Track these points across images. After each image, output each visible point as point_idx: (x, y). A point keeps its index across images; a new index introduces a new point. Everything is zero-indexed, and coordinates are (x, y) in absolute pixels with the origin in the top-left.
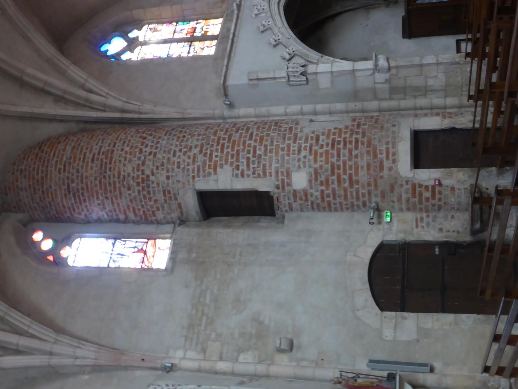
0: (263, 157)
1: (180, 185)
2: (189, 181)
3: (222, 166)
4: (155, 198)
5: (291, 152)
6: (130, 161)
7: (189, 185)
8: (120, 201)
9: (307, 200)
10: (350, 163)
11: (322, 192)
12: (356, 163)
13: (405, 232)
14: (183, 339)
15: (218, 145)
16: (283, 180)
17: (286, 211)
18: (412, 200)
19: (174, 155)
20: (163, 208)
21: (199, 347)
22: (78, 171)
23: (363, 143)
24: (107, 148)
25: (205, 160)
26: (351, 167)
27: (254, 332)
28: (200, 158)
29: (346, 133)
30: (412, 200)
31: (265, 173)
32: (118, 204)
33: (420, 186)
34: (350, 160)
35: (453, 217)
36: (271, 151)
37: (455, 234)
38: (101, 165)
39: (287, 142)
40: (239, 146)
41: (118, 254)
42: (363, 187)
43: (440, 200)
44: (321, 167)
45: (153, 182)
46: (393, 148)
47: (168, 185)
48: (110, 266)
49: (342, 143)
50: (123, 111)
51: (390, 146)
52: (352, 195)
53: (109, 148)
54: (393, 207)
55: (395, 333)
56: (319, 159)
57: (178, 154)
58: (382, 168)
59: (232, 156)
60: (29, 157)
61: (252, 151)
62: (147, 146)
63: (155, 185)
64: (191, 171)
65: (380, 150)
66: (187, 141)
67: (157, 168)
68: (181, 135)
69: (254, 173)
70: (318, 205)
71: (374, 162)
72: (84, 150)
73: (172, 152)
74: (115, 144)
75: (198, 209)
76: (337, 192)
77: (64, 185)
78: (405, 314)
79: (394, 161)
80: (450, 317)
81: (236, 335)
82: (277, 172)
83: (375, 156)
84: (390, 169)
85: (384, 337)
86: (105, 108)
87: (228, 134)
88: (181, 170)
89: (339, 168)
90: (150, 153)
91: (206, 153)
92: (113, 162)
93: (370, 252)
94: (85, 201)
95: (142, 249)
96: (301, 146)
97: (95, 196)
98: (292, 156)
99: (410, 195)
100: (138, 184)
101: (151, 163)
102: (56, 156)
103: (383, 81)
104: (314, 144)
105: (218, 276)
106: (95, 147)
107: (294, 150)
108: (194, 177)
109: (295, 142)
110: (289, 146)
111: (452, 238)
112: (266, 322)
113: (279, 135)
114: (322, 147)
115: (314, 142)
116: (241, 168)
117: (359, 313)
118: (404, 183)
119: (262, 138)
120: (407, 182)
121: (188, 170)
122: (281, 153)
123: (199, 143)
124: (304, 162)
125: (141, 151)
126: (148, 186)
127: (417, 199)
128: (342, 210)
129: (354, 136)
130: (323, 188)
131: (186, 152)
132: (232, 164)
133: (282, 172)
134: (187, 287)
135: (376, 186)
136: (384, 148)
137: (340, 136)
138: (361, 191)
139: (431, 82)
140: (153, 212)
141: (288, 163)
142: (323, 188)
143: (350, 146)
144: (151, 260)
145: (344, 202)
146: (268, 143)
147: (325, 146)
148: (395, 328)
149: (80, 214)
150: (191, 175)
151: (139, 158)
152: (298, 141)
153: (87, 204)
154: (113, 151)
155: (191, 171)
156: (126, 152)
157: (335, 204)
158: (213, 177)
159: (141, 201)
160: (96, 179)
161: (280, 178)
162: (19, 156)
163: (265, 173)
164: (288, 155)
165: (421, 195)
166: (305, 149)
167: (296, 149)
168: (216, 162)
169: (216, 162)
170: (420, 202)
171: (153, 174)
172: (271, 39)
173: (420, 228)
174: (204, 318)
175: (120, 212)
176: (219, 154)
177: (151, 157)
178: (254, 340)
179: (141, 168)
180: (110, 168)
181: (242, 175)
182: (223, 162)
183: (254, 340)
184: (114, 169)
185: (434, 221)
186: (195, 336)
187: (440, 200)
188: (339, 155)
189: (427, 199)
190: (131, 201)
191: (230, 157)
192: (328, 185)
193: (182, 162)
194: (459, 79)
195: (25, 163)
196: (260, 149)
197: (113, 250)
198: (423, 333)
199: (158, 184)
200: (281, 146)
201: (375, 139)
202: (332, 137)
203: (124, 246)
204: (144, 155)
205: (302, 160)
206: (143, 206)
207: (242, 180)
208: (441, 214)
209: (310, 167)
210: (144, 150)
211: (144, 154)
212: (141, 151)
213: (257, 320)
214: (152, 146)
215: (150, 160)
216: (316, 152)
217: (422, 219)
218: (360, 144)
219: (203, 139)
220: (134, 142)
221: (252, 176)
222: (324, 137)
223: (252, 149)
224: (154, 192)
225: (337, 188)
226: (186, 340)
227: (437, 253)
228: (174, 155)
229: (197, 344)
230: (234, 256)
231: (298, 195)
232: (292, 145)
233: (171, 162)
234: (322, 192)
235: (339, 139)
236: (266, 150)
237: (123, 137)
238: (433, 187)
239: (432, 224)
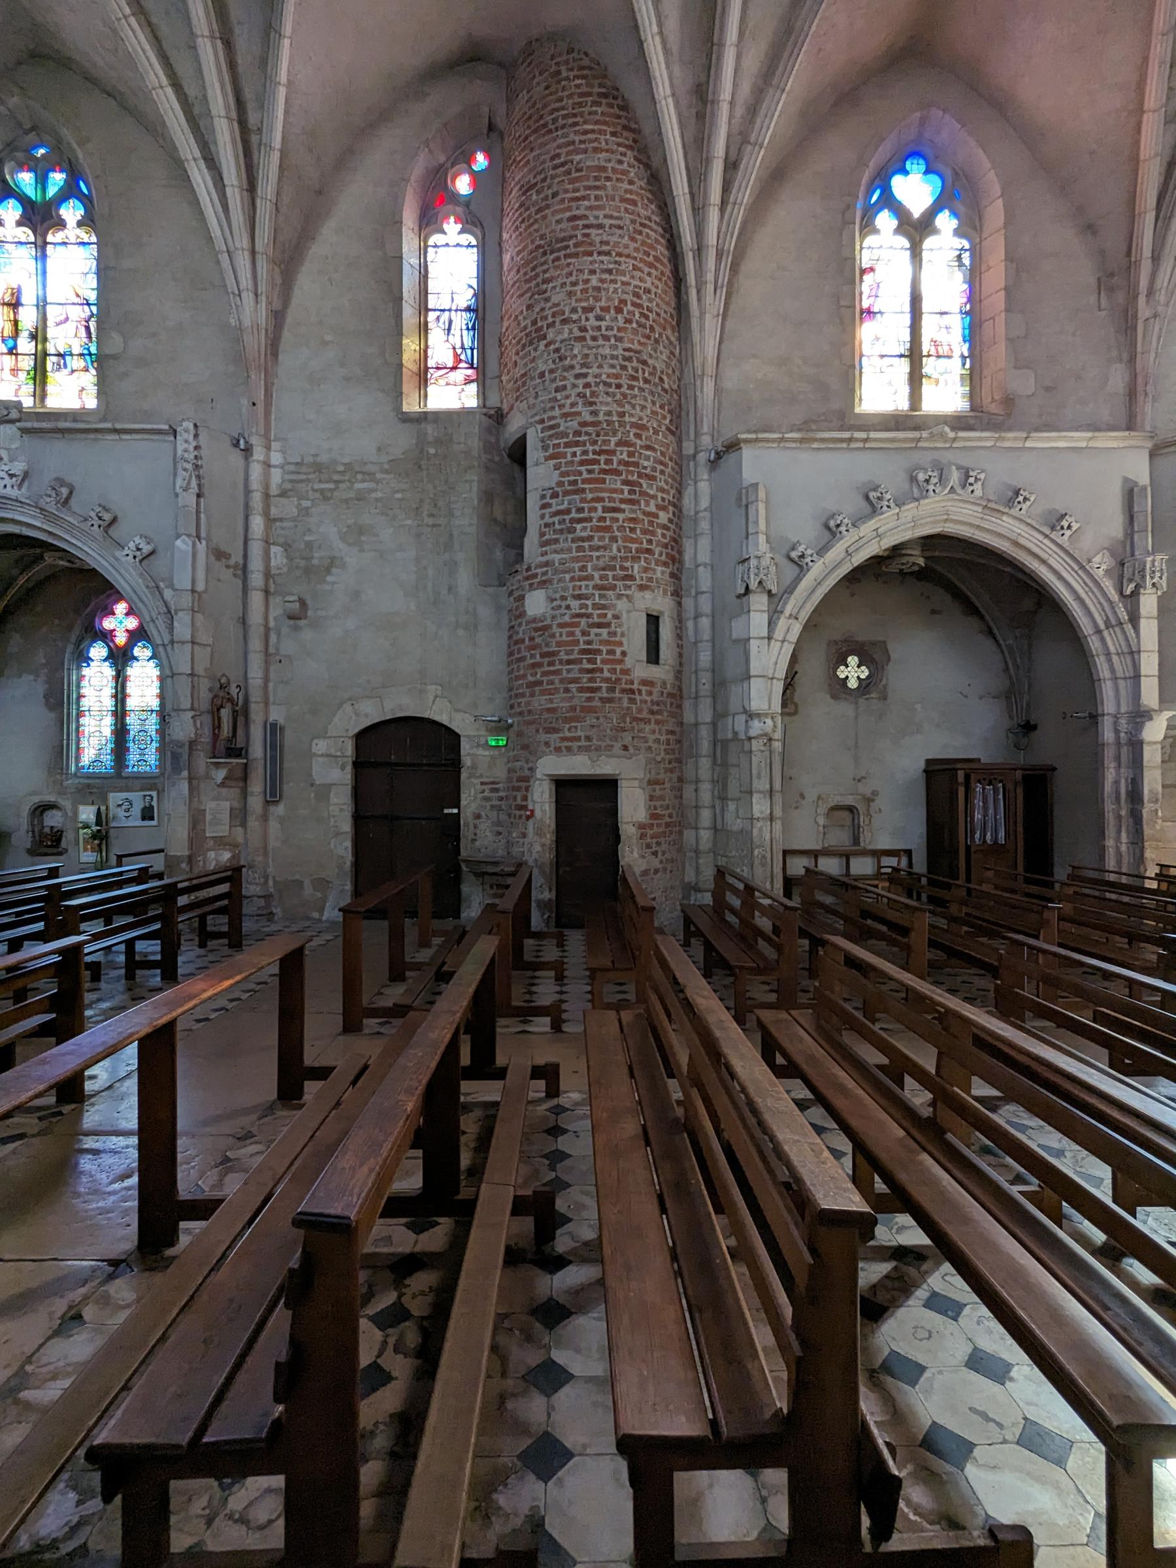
0: (570, 536)
1: (532, 401)
3: (557, 467)
5: (578, 583)
6: (570, 294)
10: (557, 681)
11: (523, 641)
12: (557, 690)
13: (474, 767)
14: (299, 460)
15: (595, 452)
19: (577, 376)
21: (288, 486)
22: (554, 195)
23: (589, 699)
24: (598, 239)
25: (567, 435)
26: (551, 682)
27: (315, 562)
29: (613, 671)
33: (527, 789)
34: (561, 681)
35: (500, 834)
36: (579, 549)
37: (471, 836)
38: (563, 239)
39: (596, 575)
40: (591, 490)
41: (450, 322)
42: (528, 703)
45: (535, 350)
46: (579, 747)
47: (532, 379)
48: (430, 313)
49: (590, 666)
50: (700, 250)
51: (583, 743)
53: (598, 245)
55: (322, 755)
56: (564, 631)
57: (581, 382)
58: (548, 731)
59: (575, 482)
60: (583, 77)
61: (582, 515)
62: (599, 318)
64: (550, 414)
65: (576, 727)
66: (607, 393)
68: (624, 381)
69: (546, 525)
71: (557, 719)
72: (593, 193)
73: (584, 371)
74: (608, 253)
76: (522, 664)
78: (349, 768)
79: (558, 750)
80: (347, 826)
81: (307, 538)
82: (547, 564)
83: (567, 720)
84: (547, 744)
85: (315, 741)
86: (698, 210)
87: (621, 468)
88: (554, 394)
90: (583, 329)
91: (580, 435)
92: (569, 260)
93: (443, 719)
95: (461, 361)
96: (587, 599)
98: (571, 585)
101: (566, 336)
102: (583, 138)
104: (590, 620)
105: (399, 496)
106: (601, 214)
107: (580, 588)
108: (542, 421)
109: (596, 587)
110: (589, 578)
111: (466, 833)
112: (329, 579)
113: (614, 558)
114: (584, 633)
115: (596, 620)
116: (554, 501)
117: (347, 707)
119: (608, 529)
120: (531, 769)
122: (577, 565)
123: (601, 417)
124: (560, 606)
125: (587, 310)
129: (604, 685)
131: (585, 396)
132: (561, 484)
134: (379, 449)
136: (579, 733)
137: (604, 662)
139: (732, 806)
141: (560, 580)
143: (585, 680)
144: (442, 382)
146: (596, 542)
147: (586, 638)
148: (328, 756)
150: (545, 416)
151: (574, 310)
152: (597, 593)
154: (590, 254)
155: (550, 414)
156: (587, 281)
158: (542, 455)
160: (542, 237)
161: (539, 571)
162: (586, 54)
164: (572, 579)
166: (582, 606)
167: (584, 591)
168: (564, 455)
169: (564, 455)
172: (840, 518)
173: (479, 787)
174: (332, 486)
176: (578, 459)
177: (577, 333)
178: (302, 563)
179: (558, 320)
180: (558, 259)
181: (544, 506)
182: (563, 469)
183: (302, 563)
184: (556, 268)
185: (492, 806)
186: (303, 477)
188: (569, 662)
191: (572, 478)
193: (564, 393)
194: (734, 853)
195: (572, 74)
196: (585, 529)
197: (456, 310)
198: (323, 792)
200: (589, 565)
201: (598, 719)
202: (604, 649)
203: (464, 327)
204: (580, 319)
205: (564, 604)
207: (537, 508)
208: (503, 817)
209: (553, 617)
210: (591, 315)
211: (583, 317)
212: (587, 310)
213: (332, 563)
214: (599, 328)
215: (571, 332)
216: (577, 625)
217: (497, 790)
218: (588, 695)
219: (609, 423)
220: (611, 290)
221: (542, 522)
222: (605, 636)
223: (585, 515)
225: (526, 663)
226: (297, 464)
227: (446, 811)
228: (577, 376)
229: (291, 481)
230: (431, 515)
232: (591, 583)
233: (565, 374)
234: (523, 641)
235: (598, 661)
236: (583, 539)
237: (623, 267)
238: (525, 808)
239: (488, 804)
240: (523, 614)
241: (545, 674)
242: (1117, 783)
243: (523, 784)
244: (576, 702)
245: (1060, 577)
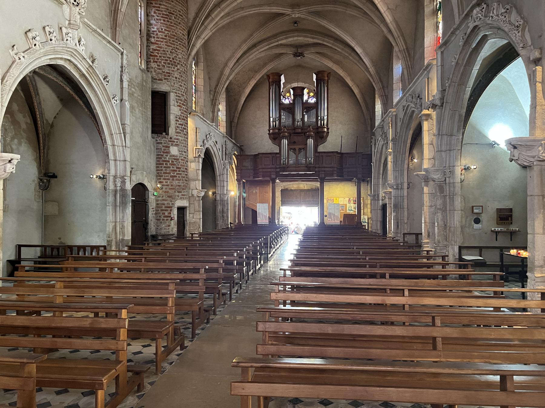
2: (174, 90)
4: (165, 66)
7: (173, 89)
8: (164, 43)
9: (164, 153)
11: (169, 161)
16: (174, 142)
17: (157, 140)
18: (164, 206)
20: (160, 69)
26: (179, 177)
28: (183, 98)
30: (164, 206)
31: (177, 133)
32: (162, 42)
33: (171, 210)
34: (182, 177)
43: (164, 220)
44: (180, 162)
52: (166, 176)
54: (159, 197)
58: (179, 192)
63: (173, 69)
67: (180, 73)
69: (177, 127)
70: (161, 158)
75: (157, 90)
77: (173, 11)
79: (181, 198)
82: (178, 139)
83: (183, 189)
84: (178, 196)
89: (179, 171)
94: (164, 21)
97: (167, 29)
99: (166, 205)
100: (173, 59)
103: (193, 193)
108: (176, 93)
118: (173, 203)
120: (173, 204)
121: (179, 91)
126: (172, 65)
127: (164, 208)
128: (157, 170)
130: (170, 162)
132: (181, 115)
133: (177, 142)
135: (171, 189)
138: (169, 181)
140: (156, 62)
142: (170, 162)
145: (162, 172)
149: (155, 13)
150: (177, 92)
157: (161, 167)
158: (176, 104)
159: (164, 57)
163: (177, 133)
165: (166, 210)
170: (162, 210)
171: (178, 69)
175: (157, 41)
187: (164, 220)
188: (183, 171)
189: (164, 214)
192: (172, 165)
199: (173, 71)
206: (160, 57)
224: (169, 67)
231: (167, 148)
234: (169, 161)
238: (170, 216)
240: (169, 152)
241: (177, 174)
242: (220, 209)
243: (169, 209)
244: (185, 184)
245: (217, 162)
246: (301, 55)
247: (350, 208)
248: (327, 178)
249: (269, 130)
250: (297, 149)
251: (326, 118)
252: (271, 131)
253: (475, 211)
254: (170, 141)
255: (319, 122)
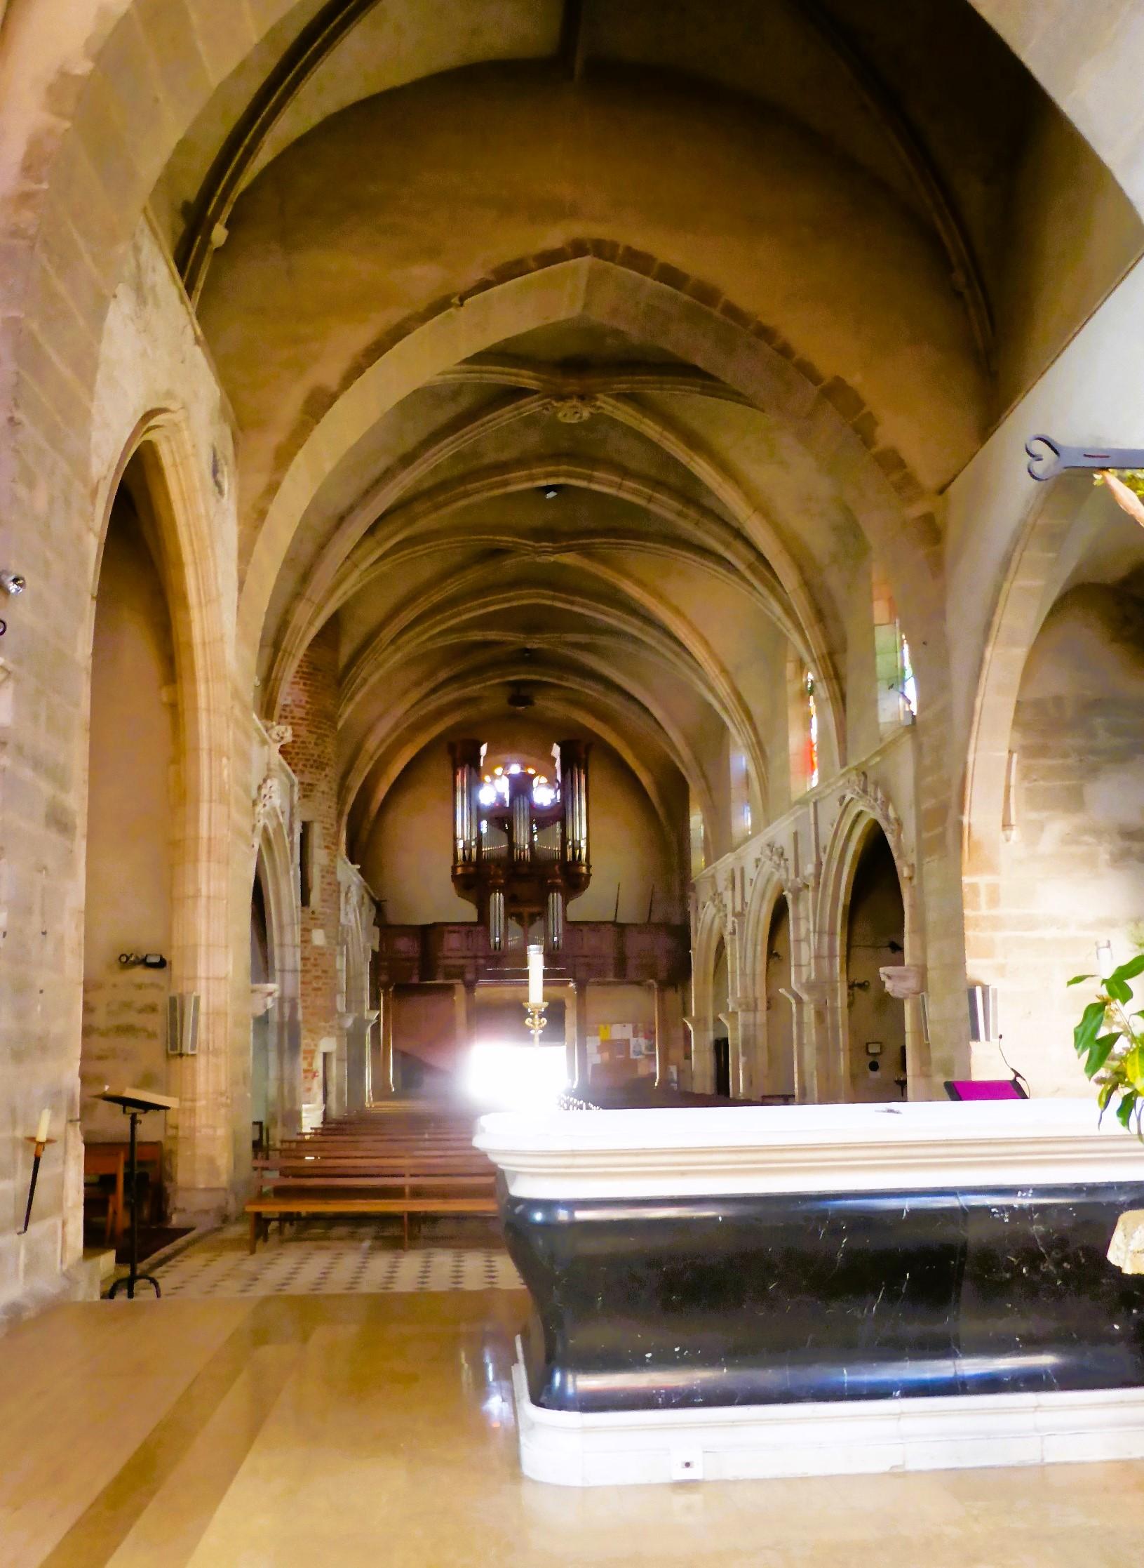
84: (325, 1028)
108: (323, 822)
126: (317, 768)
130: (312, 960)
142: (312, 960)
153: (301, 686)
158: (323, 844)
159: (303, 754)
161: (322, 917)
171: (326, 776)
190: (303, 742)
199: (318, 780)
206: (297, 754)
241: (324, 984)
246: (527, 701)
247: (637, 1049)
248: (592, 980)
249: (454, 868)
250: (525, 915)
251: (583, 844)
252: (459, 871)
253: (871, 1051)
254: (312, 919)
255: (569, 852)
